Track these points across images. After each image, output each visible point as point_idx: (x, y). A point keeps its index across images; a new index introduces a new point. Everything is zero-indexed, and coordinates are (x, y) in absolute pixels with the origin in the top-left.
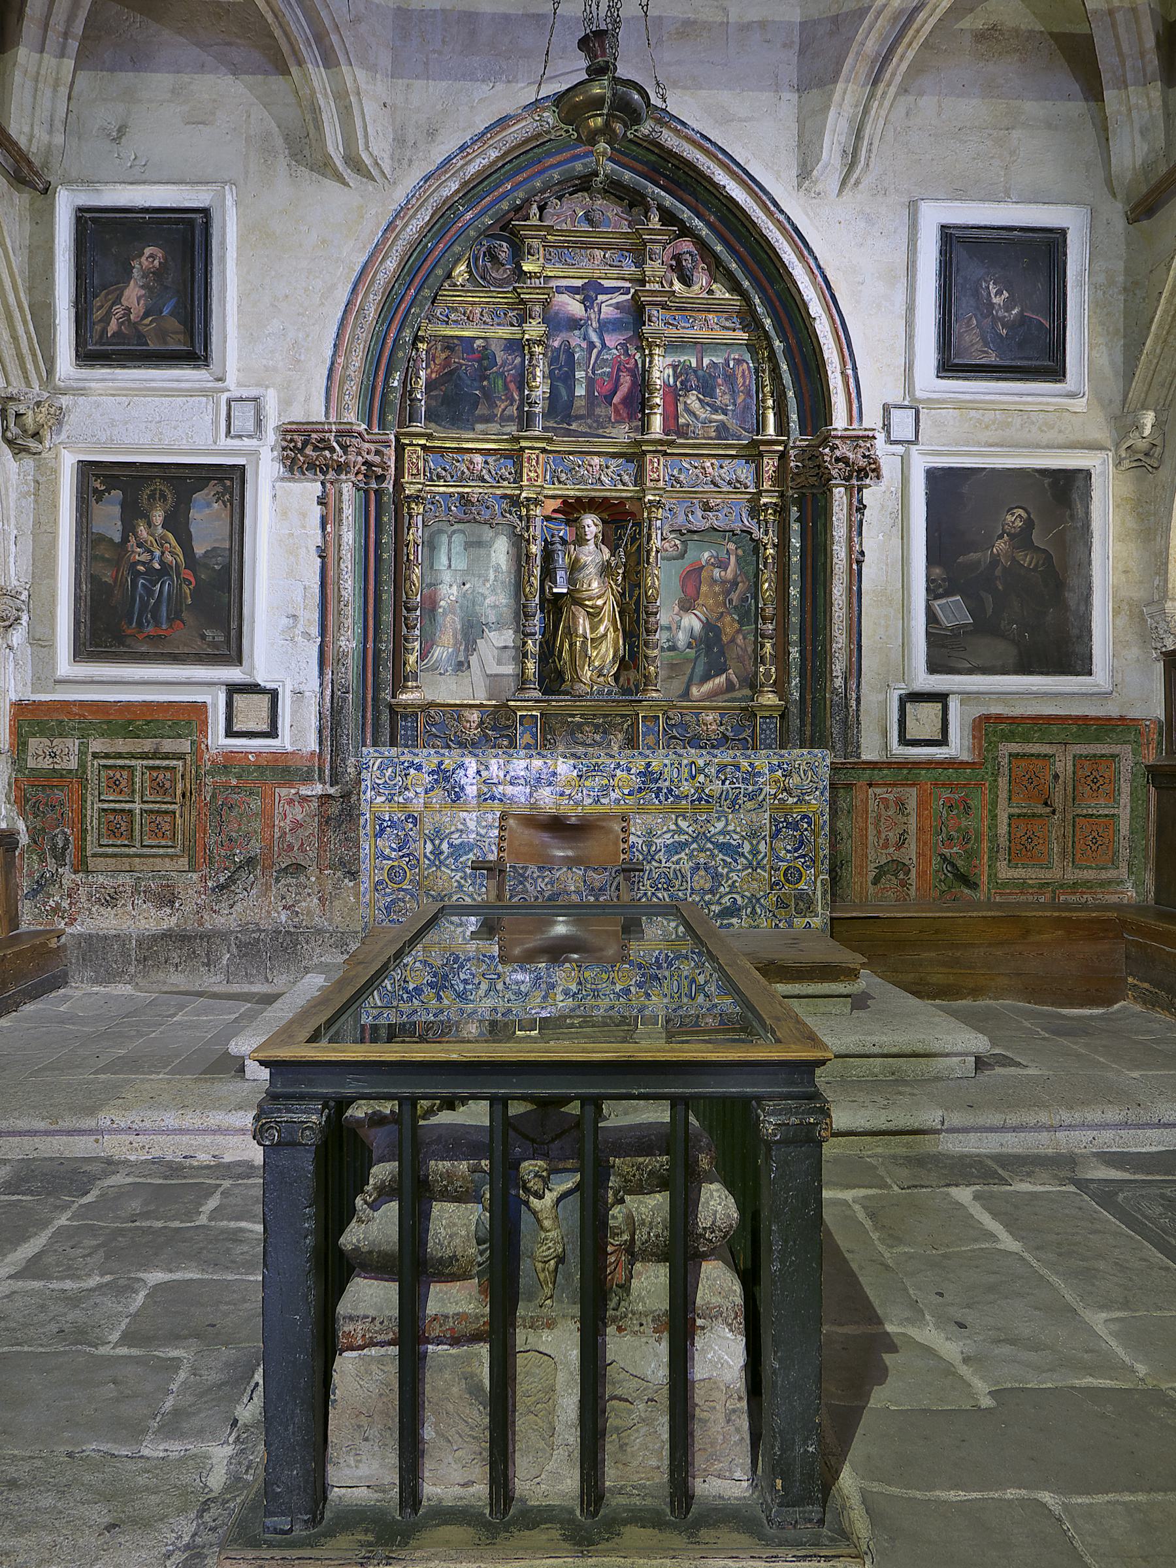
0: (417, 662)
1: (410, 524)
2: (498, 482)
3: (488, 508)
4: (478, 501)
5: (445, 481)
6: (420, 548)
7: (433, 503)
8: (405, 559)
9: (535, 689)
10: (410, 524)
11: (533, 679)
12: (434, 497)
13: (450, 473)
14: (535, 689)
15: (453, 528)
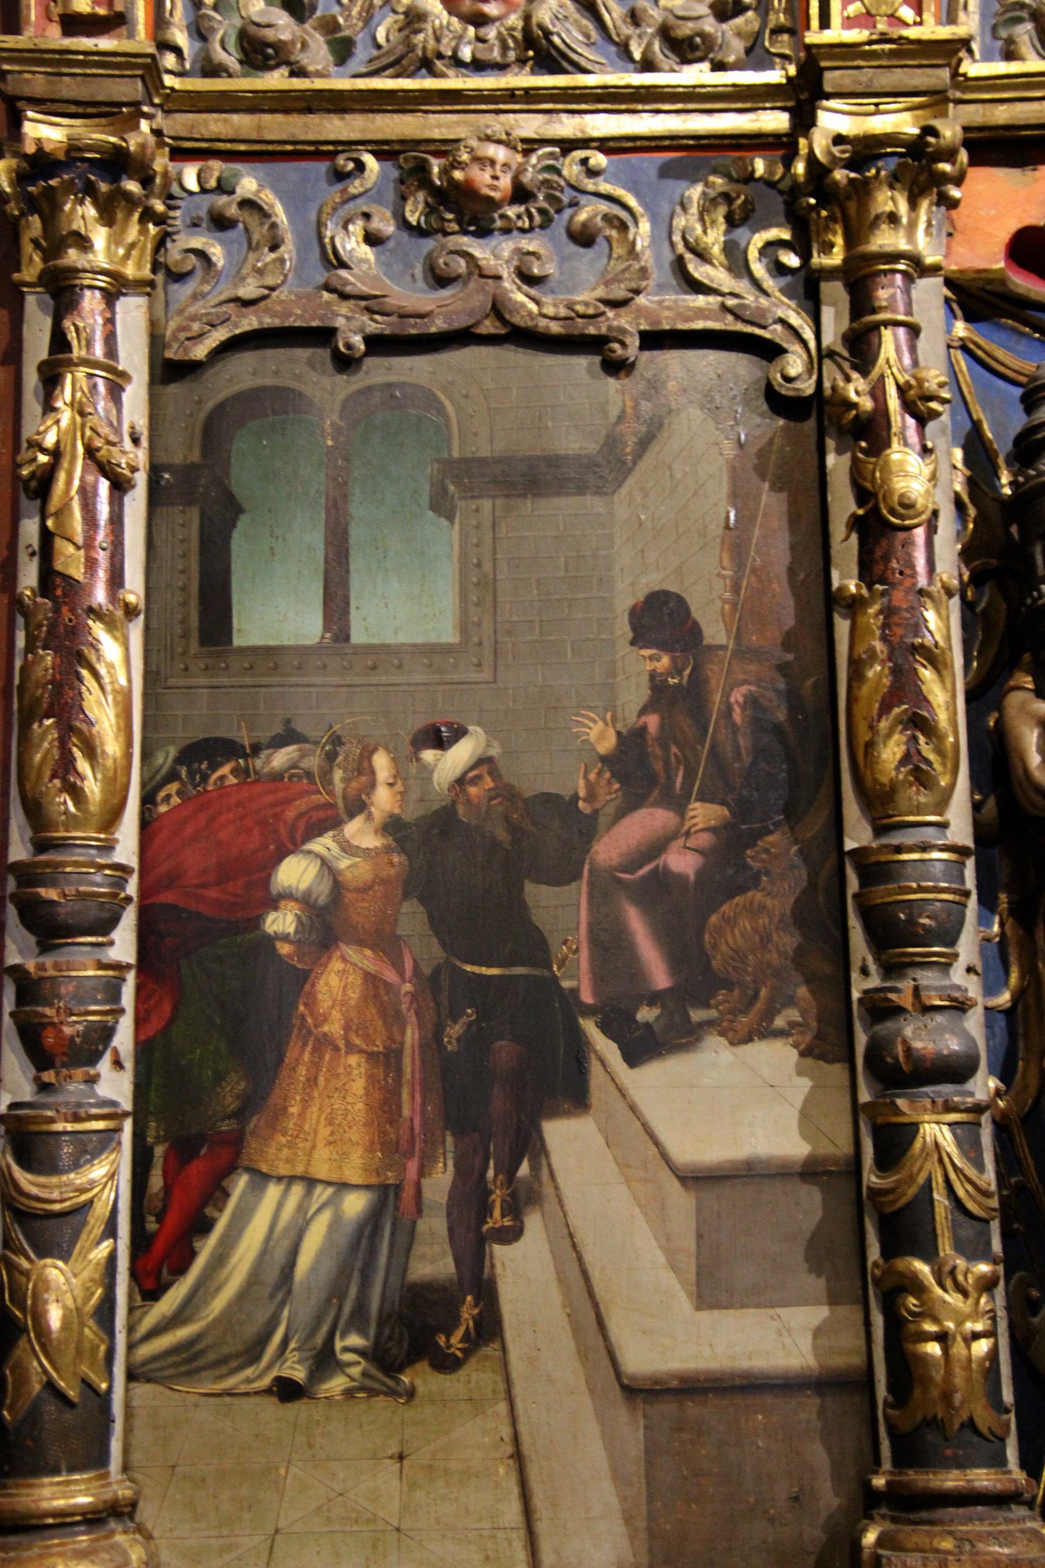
0: (105, 1312)
1: (59, 342)
2: (648, 65)
3: (584, 238)
4: (521, 194)
5: (299, 72)
6: (136, 503)
7: (220, 223)
8: (29, 576)
9: (1000, 1500)
10: (59, 342)
11: (984, 1418)
12: (224, 188)
13: (330, 27)
14: (1000, 1500)
15: (358, 381)
